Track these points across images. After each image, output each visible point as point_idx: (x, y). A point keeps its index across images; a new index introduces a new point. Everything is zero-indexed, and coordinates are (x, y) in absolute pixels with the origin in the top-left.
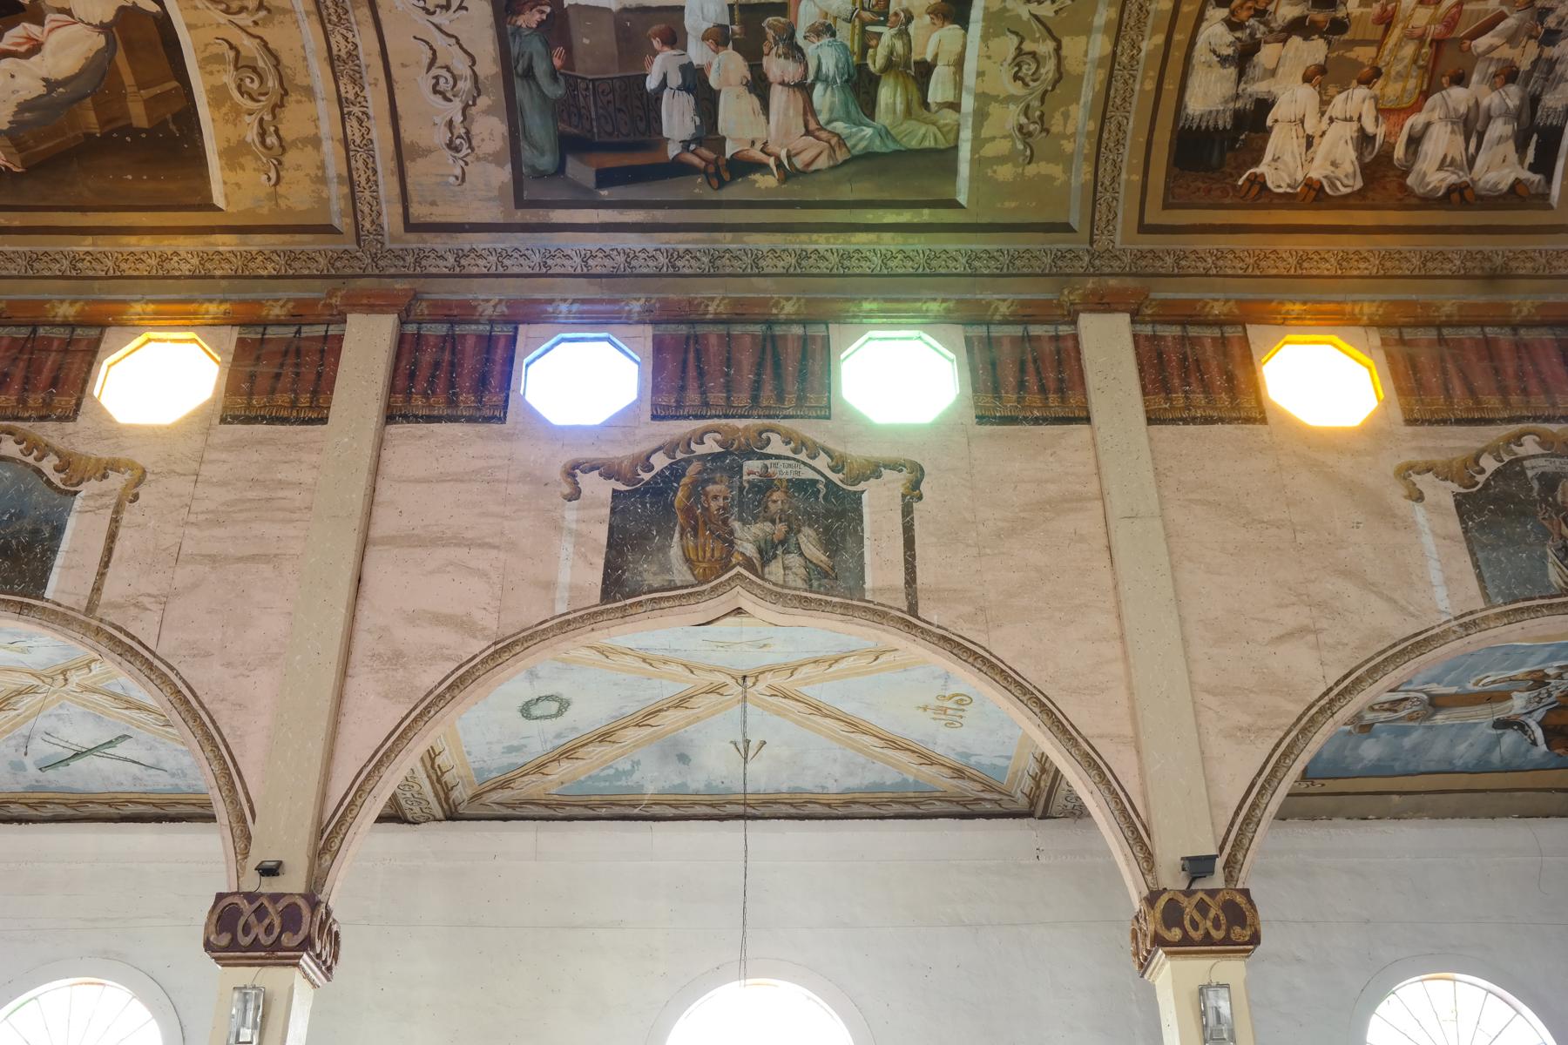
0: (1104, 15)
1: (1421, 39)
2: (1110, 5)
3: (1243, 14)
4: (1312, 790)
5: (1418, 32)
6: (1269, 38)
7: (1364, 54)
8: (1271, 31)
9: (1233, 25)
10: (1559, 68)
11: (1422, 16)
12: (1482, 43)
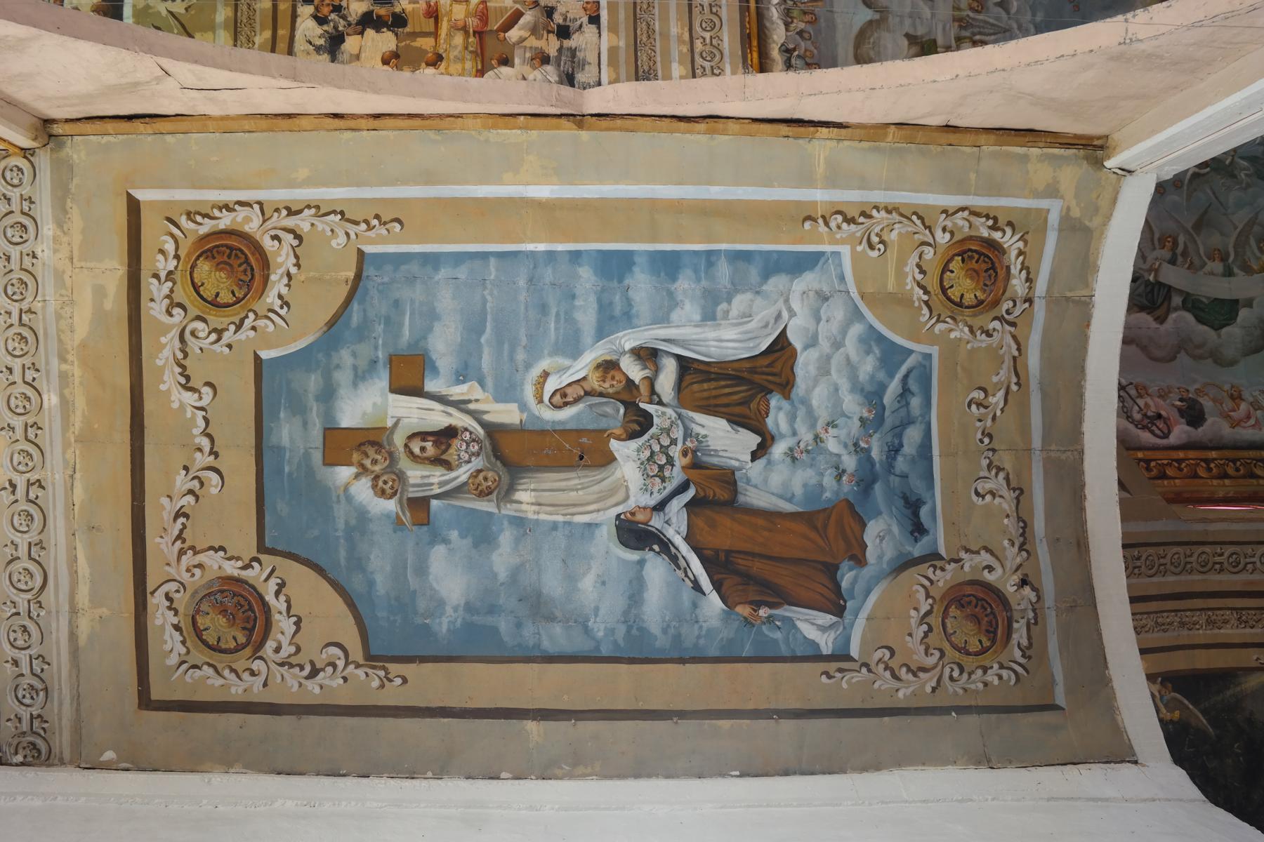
0: (223, 14)
1: (464, 29)
2: (226, 5)
3: (325, 10)
4: (393, 695)
5: (461, 24)
6: (350, 30)
7: (426, 43)
8: (350, 25)
9: (321, 20)
10: (580, 55)
11: (459, 12)
12: (514, 34)
